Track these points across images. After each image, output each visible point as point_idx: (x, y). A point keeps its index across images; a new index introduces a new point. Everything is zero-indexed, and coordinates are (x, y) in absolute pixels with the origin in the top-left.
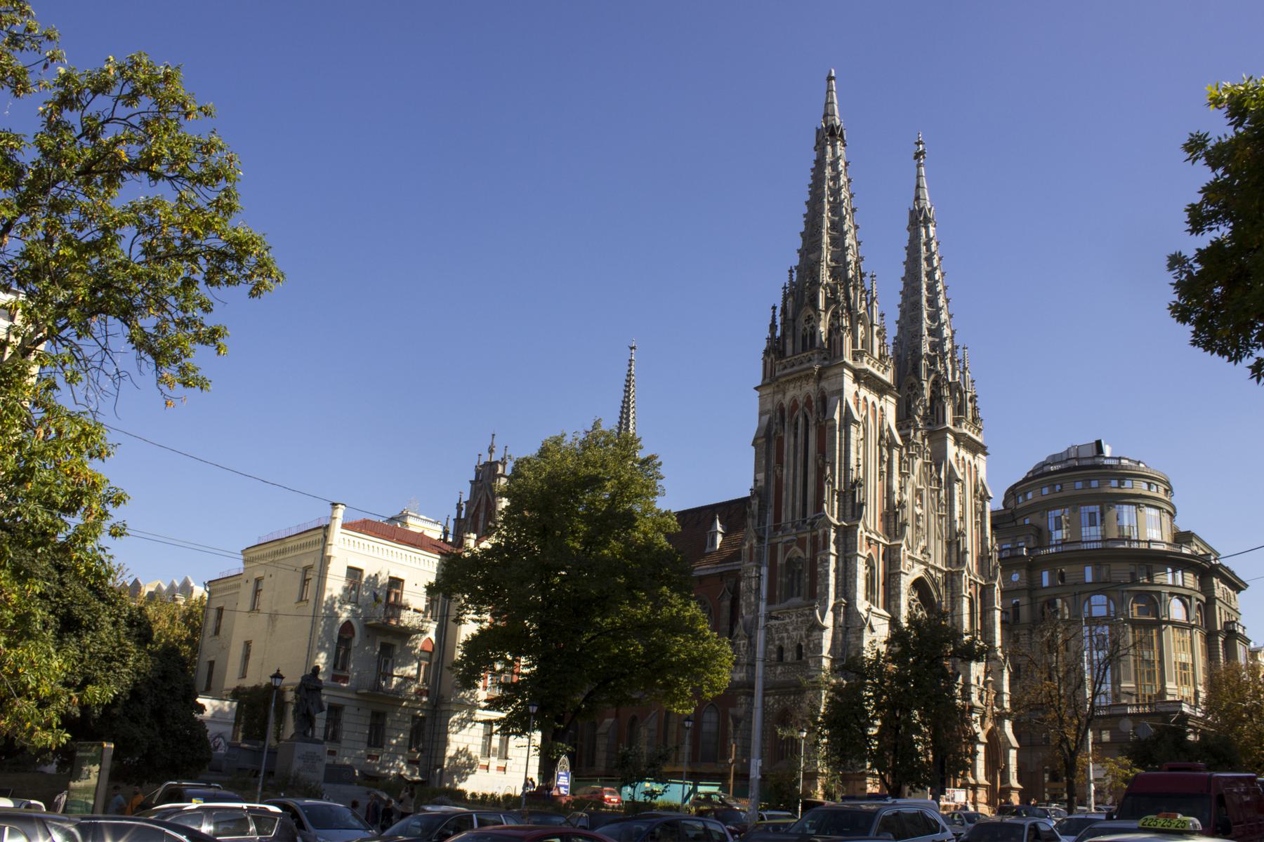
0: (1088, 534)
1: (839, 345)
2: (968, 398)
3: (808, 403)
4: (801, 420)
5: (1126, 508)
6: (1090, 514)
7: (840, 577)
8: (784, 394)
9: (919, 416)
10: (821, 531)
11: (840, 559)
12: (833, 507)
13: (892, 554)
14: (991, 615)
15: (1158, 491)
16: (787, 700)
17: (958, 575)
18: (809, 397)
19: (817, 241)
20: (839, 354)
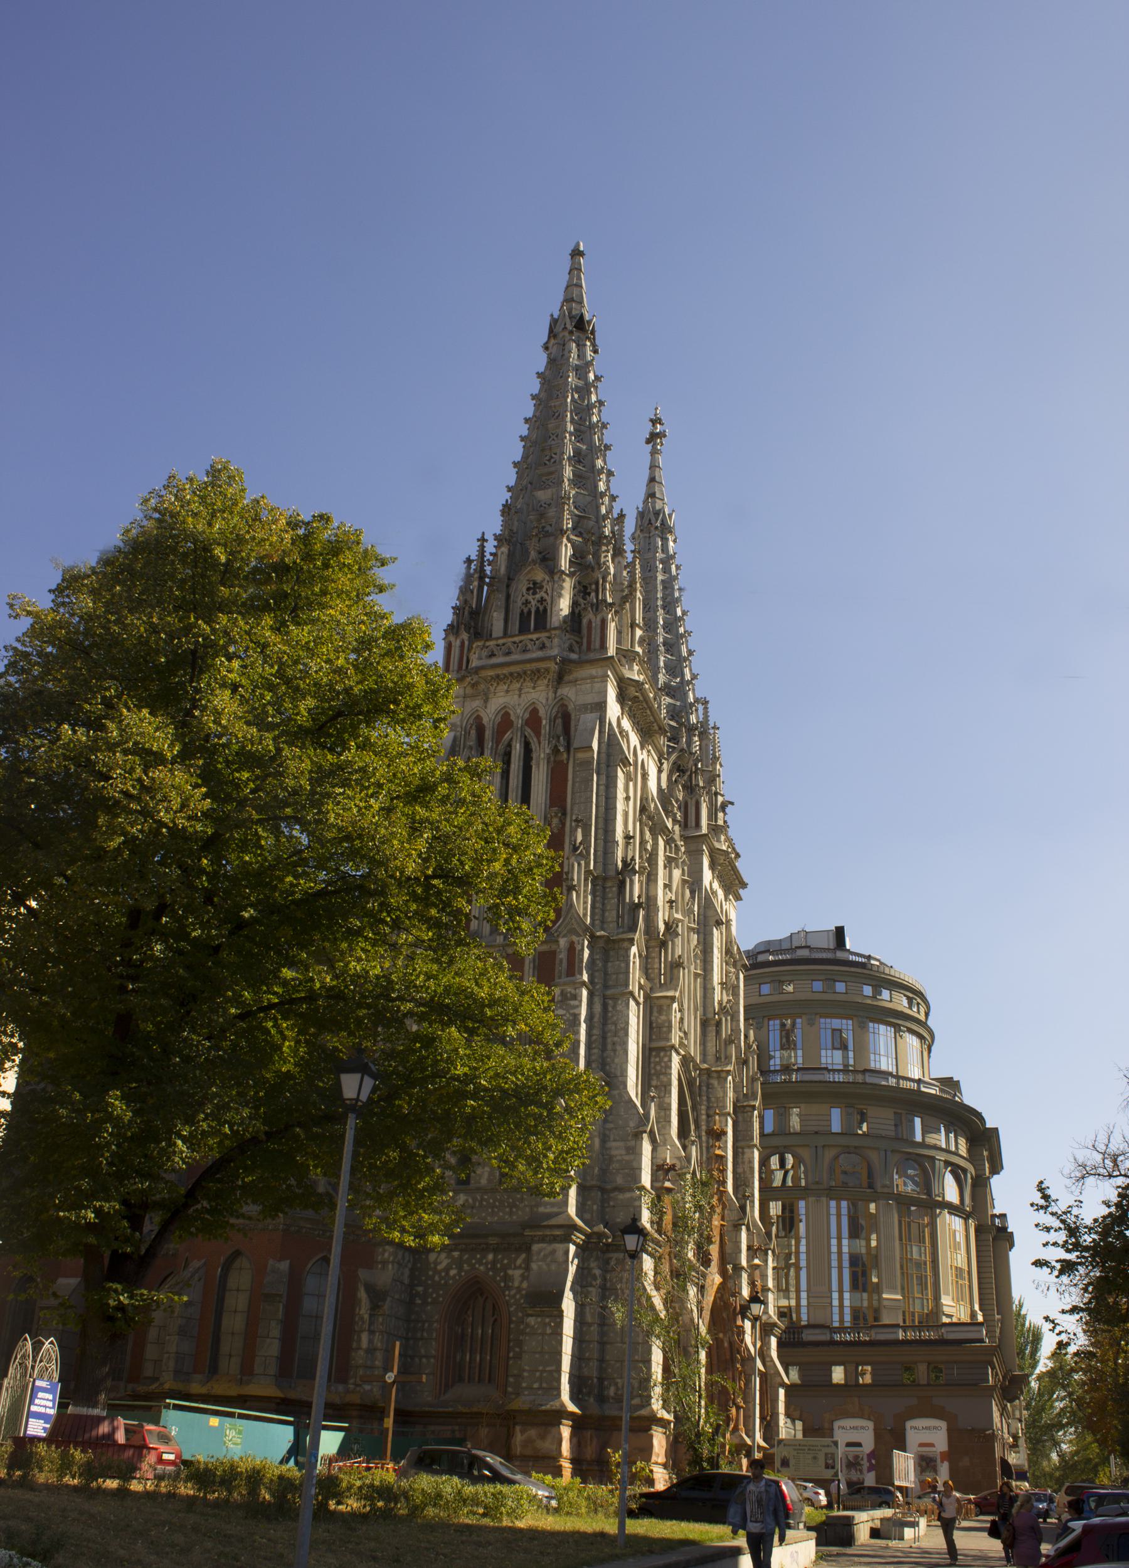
0: (830, 1061)
1: (599, 631)
2: (719, 804)
3: (533, 720)
4: (517, 748)
5: (882, 1028)
6: (834, 1030)
7: (595, 1032)
8: (486, 701)
9: (677, 801)
10: (563, 942)
11: (596, 999)
12: (585, 903)
13: (655, 1014)
14: (746, 1156)
15: (919, 1012)
16: (480, 1262)
17: (719, 1077)
18: (534, 712)
19: (551, 473)
20: (597, 645)
